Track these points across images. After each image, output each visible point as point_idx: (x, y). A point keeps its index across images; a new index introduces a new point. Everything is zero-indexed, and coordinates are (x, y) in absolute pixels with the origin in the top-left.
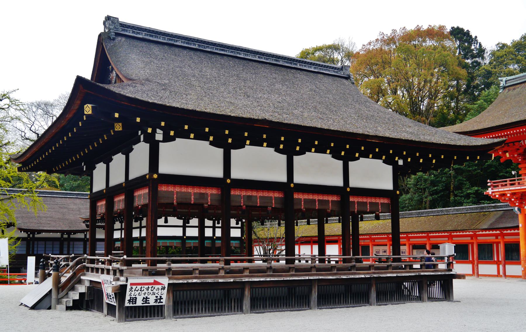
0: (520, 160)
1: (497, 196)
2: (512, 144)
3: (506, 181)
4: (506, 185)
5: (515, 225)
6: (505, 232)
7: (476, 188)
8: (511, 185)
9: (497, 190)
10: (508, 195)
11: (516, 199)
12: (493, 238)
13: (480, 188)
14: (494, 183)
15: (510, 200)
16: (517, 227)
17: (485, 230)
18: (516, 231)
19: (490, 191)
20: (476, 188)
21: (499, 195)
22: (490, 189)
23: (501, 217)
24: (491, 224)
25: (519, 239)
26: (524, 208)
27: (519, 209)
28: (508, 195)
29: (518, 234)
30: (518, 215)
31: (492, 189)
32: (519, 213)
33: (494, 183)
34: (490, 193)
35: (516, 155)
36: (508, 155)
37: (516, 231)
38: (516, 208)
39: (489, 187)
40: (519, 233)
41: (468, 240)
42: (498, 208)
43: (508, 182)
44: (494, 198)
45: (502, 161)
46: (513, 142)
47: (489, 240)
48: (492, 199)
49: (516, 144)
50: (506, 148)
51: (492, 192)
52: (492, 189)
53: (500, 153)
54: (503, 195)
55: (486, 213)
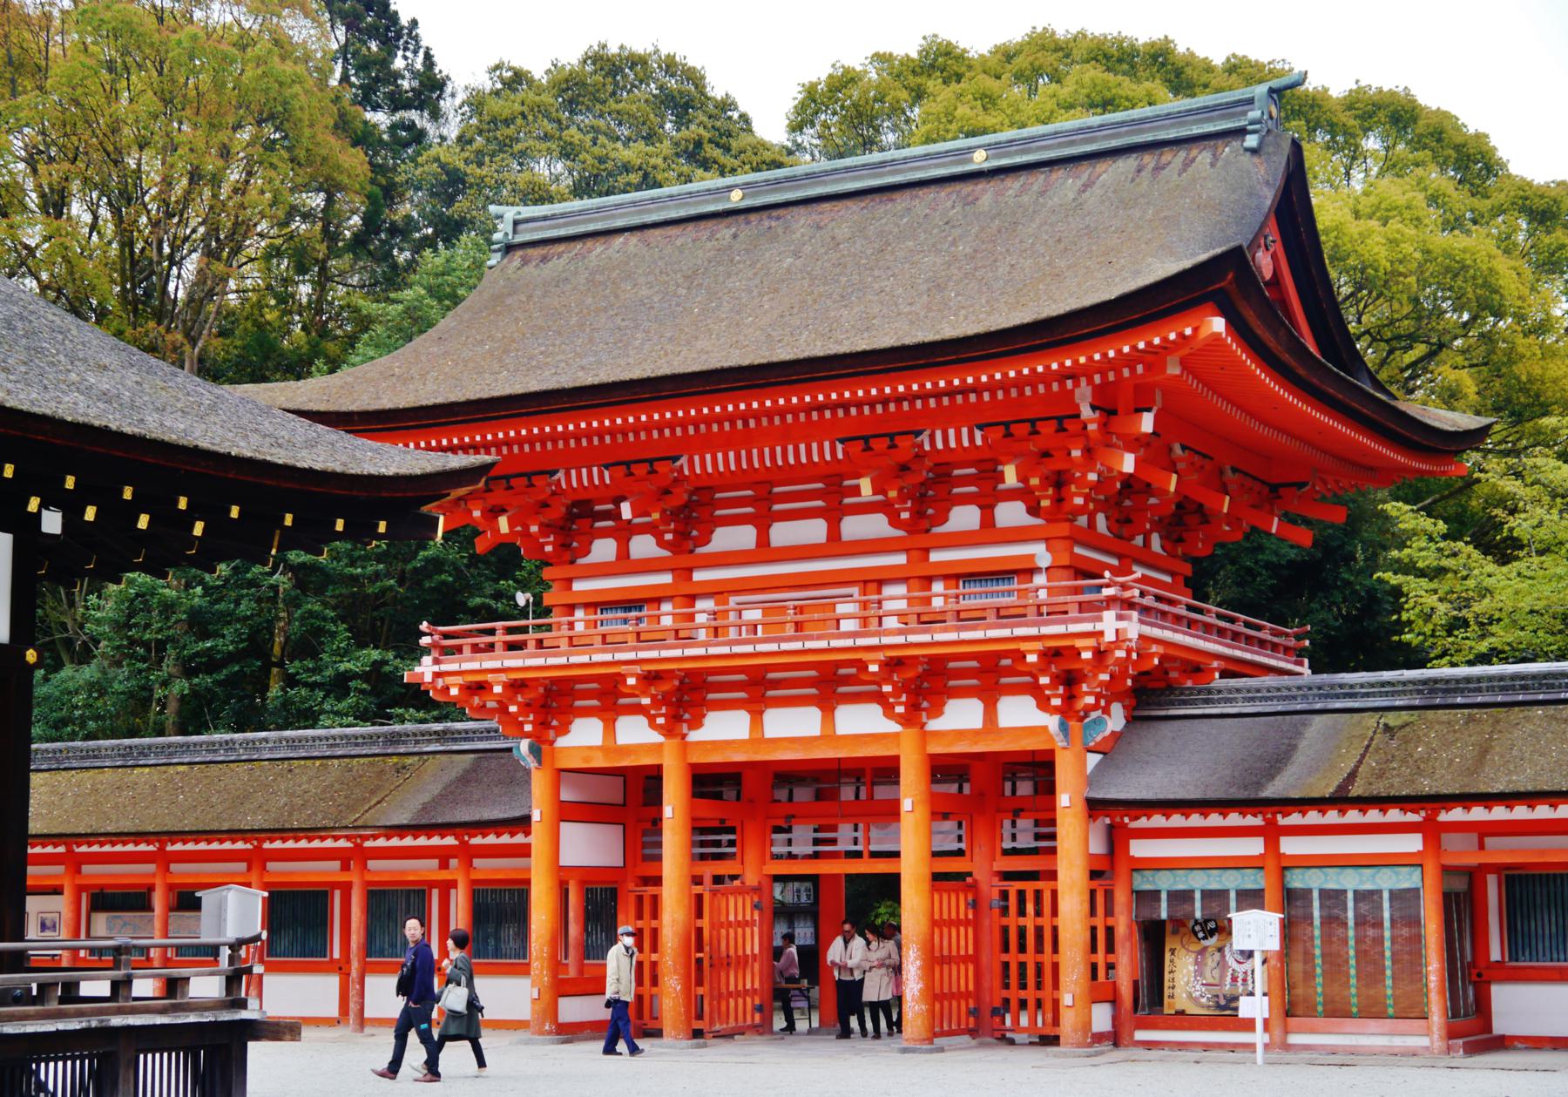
0: (549, 548)
1: (454, 691)
2: (525, 481)
3: (492, 632)
4: (491, 647)
5: (517, 813)
7: (375, 655)
8: (511, 647)
9: (454, 667)
10: (498, 689)
11: (526, 707)
12: (427, 868)
13: (390, 655)
14: (446, 636)
15: (503, 709)
17: (401, 830)
18: (519, 839)
19: (425, 669)
20: (375, 655)
21: (462, 688)
22: (427, 660)
23: (465, 779)
24: (425, 808)
25: (529, 870)
26: (552, 743)
27: (535, 751)
28: (498, 689)
29: (524, 851)
30: (528, 772)
31: (436, 662)
32: (531, 763)
33: (446, 636)
34: (428, 678)
35: (534, 529)
36: (503, 523)
37: (519, 839)
38: (524, 745)
39: (426, 651)
40: (529, 845)
41: (326, 873)
42: (455, 740)
43: (499, 638)
44: (438, 698)
45: (481, 546)
46: (528, 475)
47: (415, 872)
48: (434, 704)
49: (538, 481)
51: (437, 675)
53: (477, 514)
54: (481, 688)
55: (409, 761)
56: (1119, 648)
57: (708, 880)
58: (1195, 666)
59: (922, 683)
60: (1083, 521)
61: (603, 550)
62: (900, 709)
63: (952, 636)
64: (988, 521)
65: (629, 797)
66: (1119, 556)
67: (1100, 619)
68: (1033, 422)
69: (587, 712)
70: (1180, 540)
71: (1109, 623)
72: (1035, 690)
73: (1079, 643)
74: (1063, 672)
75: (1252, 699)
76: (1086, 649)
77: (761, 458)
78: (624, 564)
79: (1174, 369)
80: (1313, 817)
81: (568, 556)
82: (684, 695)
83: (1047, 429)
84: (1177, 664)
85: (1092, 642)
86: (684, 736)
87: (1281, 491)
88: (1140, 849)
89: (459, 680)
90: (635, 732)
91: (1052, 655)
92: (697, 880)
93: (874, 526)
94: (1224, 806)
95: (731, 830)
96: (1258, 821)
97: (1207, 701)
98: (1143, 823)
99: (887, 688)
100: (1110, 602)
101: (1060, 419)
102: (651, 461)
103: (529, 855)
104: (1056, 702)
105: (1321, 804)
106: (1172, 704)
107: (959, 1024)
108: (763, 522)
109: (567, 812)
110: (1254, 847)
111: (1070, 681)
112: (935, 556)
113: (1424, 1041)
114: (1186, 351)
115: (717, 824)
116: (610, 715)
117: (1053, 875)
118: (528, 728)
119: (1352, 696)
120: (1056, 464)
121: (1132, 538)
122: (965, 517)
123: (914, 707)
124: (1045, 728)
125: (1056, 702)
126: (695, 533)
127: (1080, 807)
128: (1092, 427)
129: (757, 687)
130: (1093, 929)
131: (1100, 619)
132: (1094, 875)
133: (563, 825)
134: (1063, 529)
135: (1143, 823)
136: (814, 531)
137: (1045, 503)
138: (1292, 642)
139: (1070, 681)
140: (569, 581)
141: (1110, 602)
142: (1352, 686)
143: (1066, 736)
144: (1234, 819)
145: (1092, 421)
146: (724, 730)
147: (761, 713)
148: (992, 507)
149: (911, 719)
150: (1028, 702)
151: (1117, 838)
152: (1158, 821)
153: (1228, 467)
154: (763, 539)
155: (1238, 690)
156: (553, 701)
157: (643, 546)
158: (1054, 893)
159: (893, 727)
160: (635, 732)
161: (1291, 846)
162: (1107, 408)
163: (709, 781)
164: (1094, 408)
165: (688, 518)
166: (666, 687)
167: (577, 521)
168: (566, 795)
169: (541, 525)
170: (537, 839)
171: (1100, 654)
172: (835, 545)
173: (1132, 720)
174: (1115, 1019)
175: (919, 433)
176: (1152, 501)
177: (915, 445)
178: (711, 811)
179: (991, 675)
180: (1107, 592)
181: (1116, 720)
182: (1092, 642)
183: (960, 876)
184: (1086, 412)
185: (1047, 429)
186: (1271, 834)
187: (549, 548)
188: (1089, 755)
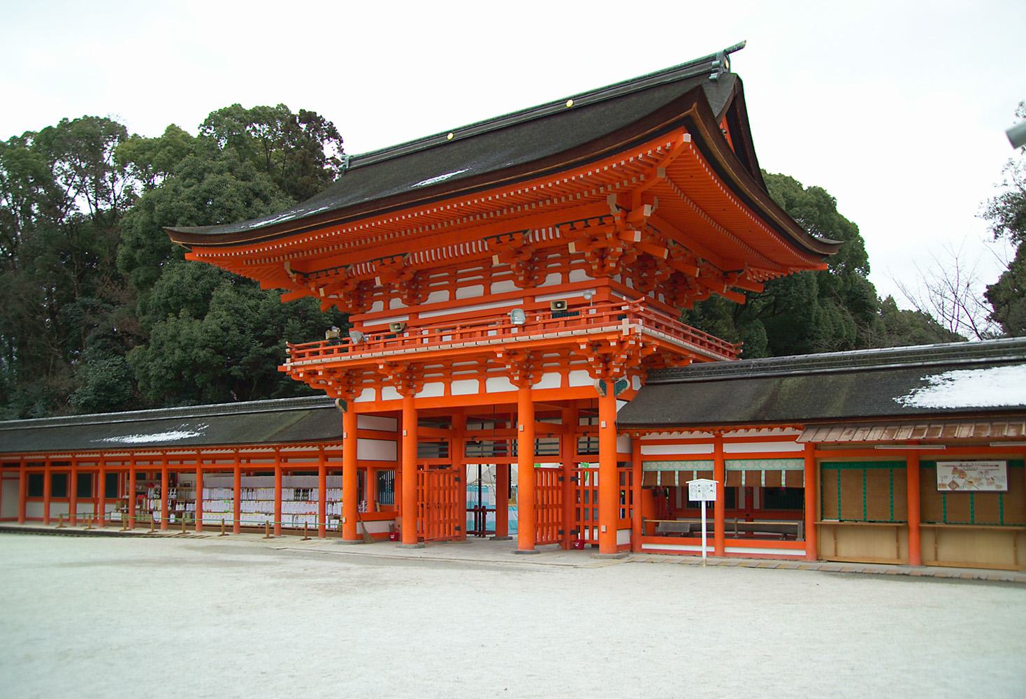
4: (317, 353)
5: (337, 435)
6: (204, 452)
8: (326, 352)
14: (299, 349)
16: (338, 439)
19: (288, 365)
33: (299, 349)
34: (289, 369)
35: (341, 296)
44: (295, 379)
50: (321, 281)
51: (293, 367)
57: (426, 468)
59: (529, 363)
61: (378, 306)
62: (516, 378)
63: (540, 337)
65: (386, 425)
69: (368, 385)
71: (625, 326)
72: (588, 367)
74: (602, 355)
76: (613, 340)
77: (448, 252)
79: (661, 175)
80: (741, 433)
81: (360, 310)
83: (594, 223)
85: (616, 337)
86: (413, 396)
88: (646, 450)
90: (391, 394)
91: (595, 345)
92: (419, 467)
93: (508, 286)
94: (691, 426)
96: (711, 436)
98: (647, 437)
99: (508, 367)
102: (392, 257)
103: (342, 456)
104: (599, 372)
105: (745, 424)
107: (553, 538)
108: (452, 289)
109: (360, 434)
110: (709, 449)
111: (606, 360)
112: (537, 300)
113: (803, 553)
114: (667, 162)
115: (440, 441)
116: (379, 386)
118: (339, 393)
122: (554, 279)
123: (525, 377)
125: (599, 372)
126: (420, 296)
127: (612, 427)
128: (617, 219)
129: (448, 368)
132: (620, 464)
133: (359, 440)
134: (605, 281)
135: (647, 437)
136: (478, 290)
137: (595, 267)
139: (606, 360)
140: (362, 322)
143: (604, 390)
144: (697, 434)
146: (432, 391)
151: (635, 444)
152: (654, 436)
156: (352, 378)
157: (396, 303)
159: (516, 388)
160: (391, 394)
161: (728, 448)
162: (626, 210)
164: (618, 207)
165: (416, 286)
166: (400, 370)
167: (362, 293)
169: (345, 294)
170: (345, 447)
171: (621, 343)
172: (488, 297)
174: (631, 538)
175: (525, 232)
177: (523, 239)
178: (426, 432)
179: (565, 357)
182: (616, 337)
184: (614, 211)
185: (594, 223)
186: (718, 442)
187: (350, 306)
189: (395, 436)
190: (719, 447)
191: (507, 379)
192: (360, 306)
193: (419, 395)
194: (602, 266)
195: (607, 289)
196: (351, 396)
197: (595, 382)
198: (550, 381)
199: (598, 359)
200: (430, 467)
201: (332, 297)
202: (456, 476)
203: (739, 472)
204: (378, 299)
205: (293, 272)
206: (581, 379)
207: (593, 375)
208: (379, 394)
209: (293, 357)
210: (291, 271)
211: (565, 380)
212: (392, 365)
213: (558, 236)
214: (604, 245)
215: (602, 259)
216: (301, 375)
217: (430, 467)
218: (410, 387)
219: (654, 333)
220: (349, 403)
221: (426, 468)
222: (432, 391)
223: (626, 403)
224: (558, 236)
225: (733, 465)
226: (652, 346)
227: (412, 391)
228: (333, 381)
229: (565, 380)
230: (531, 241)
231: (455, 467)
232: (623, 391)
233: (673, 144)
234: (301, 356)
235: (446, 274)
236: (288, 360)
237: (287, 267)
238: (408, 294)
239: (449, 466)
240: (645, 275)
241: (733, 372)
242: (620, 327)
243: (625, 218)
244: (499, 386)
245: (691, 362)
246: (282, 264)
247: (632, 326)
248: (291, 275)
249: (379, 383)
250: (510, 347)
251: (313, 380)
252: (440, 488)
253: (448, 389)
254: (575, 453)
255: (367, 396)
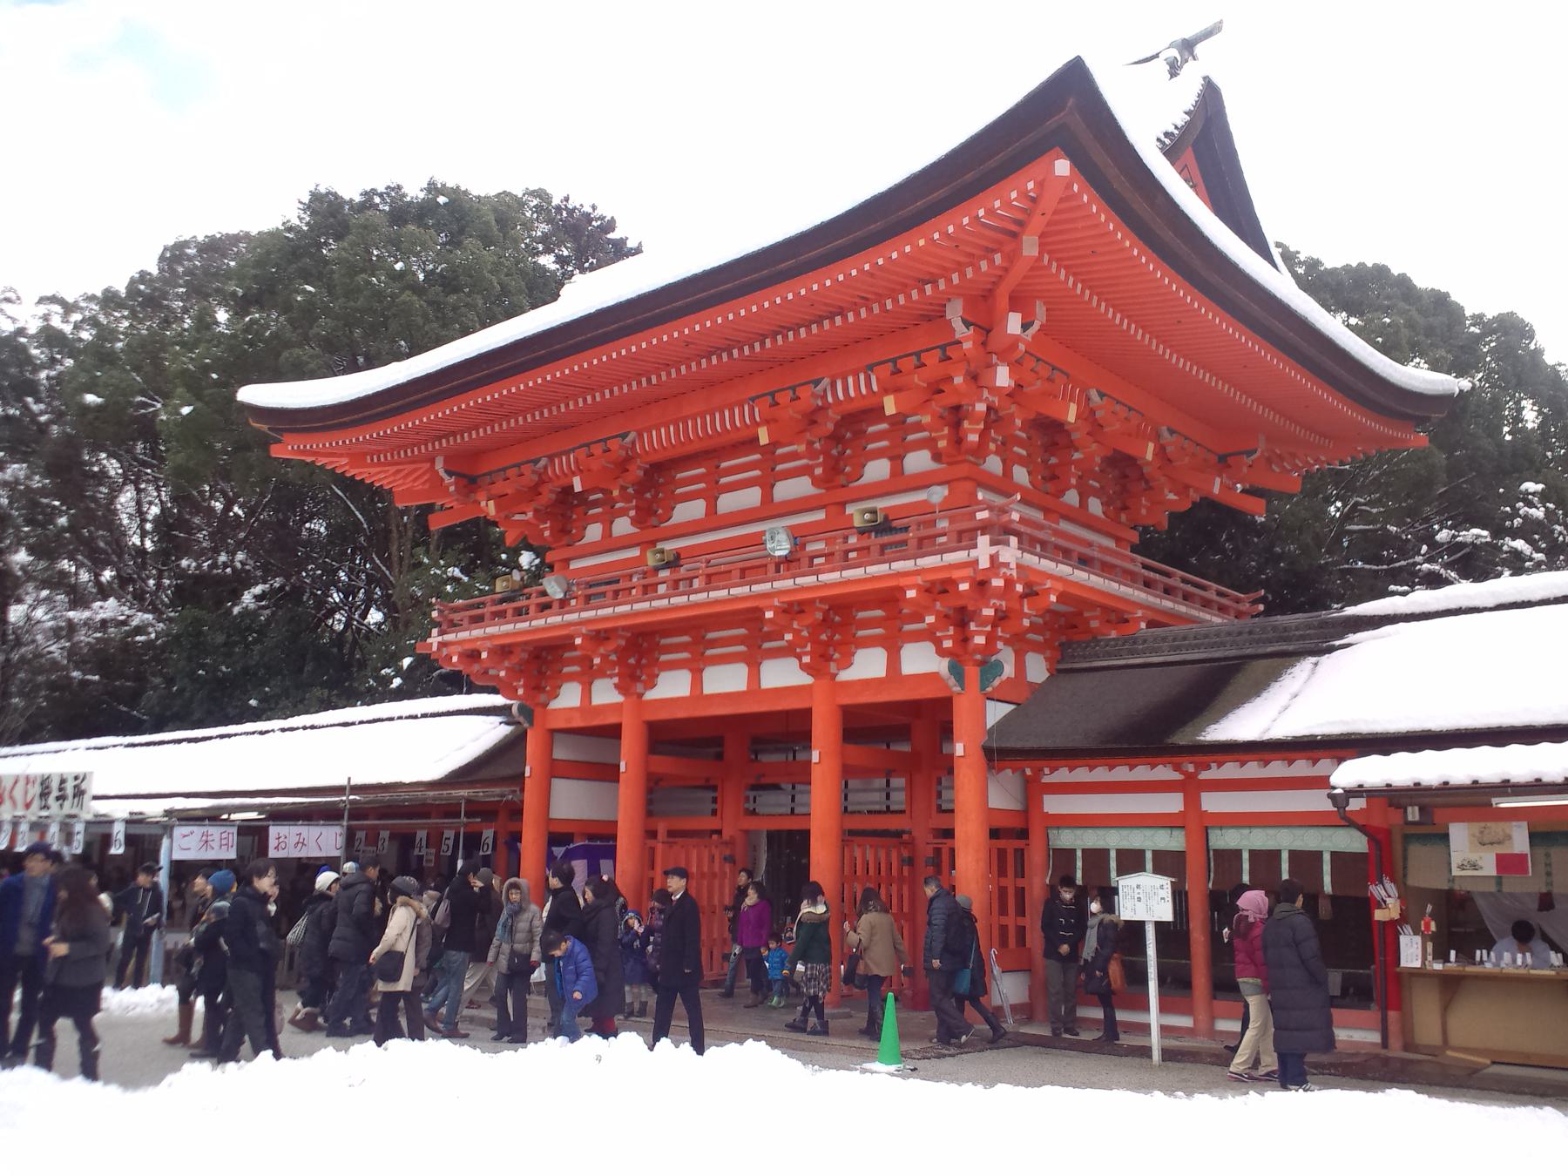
21: (461, 655)
31: (441, 633)
34: (435, 648)
35: (530, 514)
51: (442, 645)
52: (441, 633)
54: (473, 655)
56: (997, 576)
57: (661, 835)
58: (1117, 614)
60: (994, 464)
61: (594, 532)
62: (806, 659)
64: (897, 470)
66: (1047, 511)
67: (975, 546)
68: (918, 355)
69: (571, 677)
70: (1125, 508)
72: (929, 635)
73: (956, 574)
74: (954, 611)
75: (1178, 648)
76: (963, 580)
78: (609, 544)
81: (566, 540)
82: (639, 651)
83: (932, 359)
84: (1098, 612)
86: (641, 695)
87: (1230, 460)
88: (1054, 805)
89: (459, 649)
92: (652, 834)
95: (714, 788)
96: (1177, 776)
97: (1132, 653)
100: (985, 528)
101: (943, 348)
104: (948, 644)
106: (1097, 657)
109: (556, 769)
110: (1172, 803)
111: (961, 619)
114: (1038, 223)
115: (702, 783)
117: (949, 833)
119: (1287, 640)
120: (949, 399)
121: (1062, 492)
124: (934, 676)
127: (978, 757)
130: (1003, 892)
131: (975, 546)
136: (750, 497)
137: (942, 444)
138: (1245, 607)
140: (567, 561)
141: (985, 528)
142: (1285, 629)
145: (967, 338)
146: (672, 686)
147: (701, 671)
148: (902, 458)
149: (820, 665)
150: (928, 647)
151: (1033, 790)
153: (1164, 428)
154: (711, 509)
155: (1164, 639)
157: (623, 526)
158: (952, 850)
159: (807, 680)
160: (606, 693)
161: (1213, 803)
163: (672, 736)
164: (967, 324)
167: (566, 510)
168: (560, 753)
169: (536, 511)
171: (981, 585)
173: (1056, 673)
175: (817, 382)
176: (1077, 456)
177: (815, 396)
178: (663, 764)
180: (983, 515)
181: (1037, 669)
182: (969, 572)
183: (898, 834)
184: (960, 330)
185: (932, 359)
186: (1191, 788)
187: (547, 533)
188: (990, 704)
189: (608, 773)
190: (1192, 801)
191: (793, 663)
192: (564, 531)
193: (650, 695)
194: (958, 440)
195: (968, 485)
196: (542, 698)
197: (941, 666)
198: (868, 665)
199: (944, 618)
200: (672, 834)
201: (517, 517)
202: (728, 853)
203: (1237, 853)
204: (595, 519)
205: (450, 473)
206: (920, 660)
207: (941, 652)
208: (587, 694)
209: (444, 627)
210: (446, 471)
211: (894, 662)
212: (600, 636)
213: (875, 388)
214: (953, 401)
215: (956, 425)
216: (455, 659)
217: (672, 834)
218: (635, 679)
219: (1047, 565)
220: (538, 711)
221: (661, 835)
222: (672, 686)
223: (1012, 707)
224: (875, 388)
225: (1225, 839)
226: (1049, 591)
227: (639, 687)
228: (508, 669)
229: (894, 662)
230: (830, 399)
231: (726, 836)
232: (996, 682)
233: (1040, 185)
234: (454, 626)
235: (702, 470)
236: (435, 631)
237: (439, 465)
238: (637, 508)
239: (720, 832)
240: (1053, 460)
241: (1223, 644)
242: (973, 553)
243: (984, 344)
244: (782, 674)
245: (1143, 625)
246: (432, 461)
247: (994, 550)
248: (448, 480)
249: (587, 677)
250: (792, 598)
251: (476, 667)
252: (714, 875)
253: (697, 682)
254: (935, 808)
255: (569, 697)
